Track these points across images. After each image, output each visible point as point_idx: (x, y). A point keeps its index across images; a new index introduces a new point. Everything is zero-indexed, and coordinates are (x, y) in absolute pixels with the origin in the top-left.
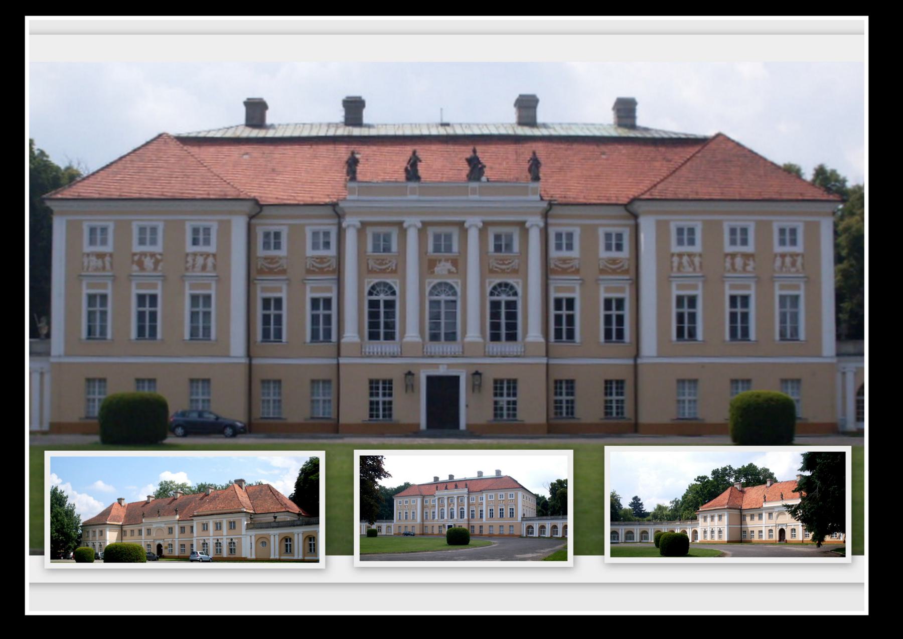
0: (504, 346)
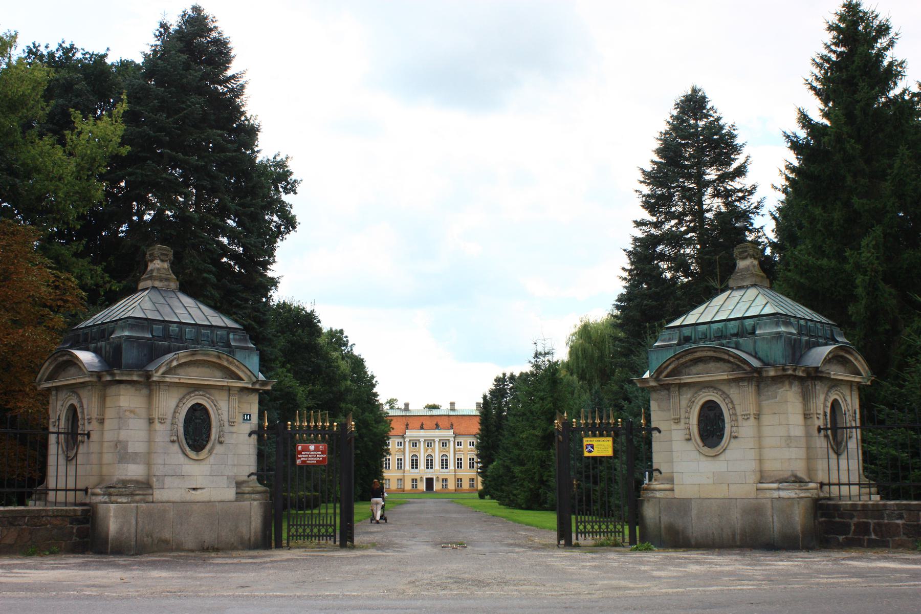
0: (444, 470)
